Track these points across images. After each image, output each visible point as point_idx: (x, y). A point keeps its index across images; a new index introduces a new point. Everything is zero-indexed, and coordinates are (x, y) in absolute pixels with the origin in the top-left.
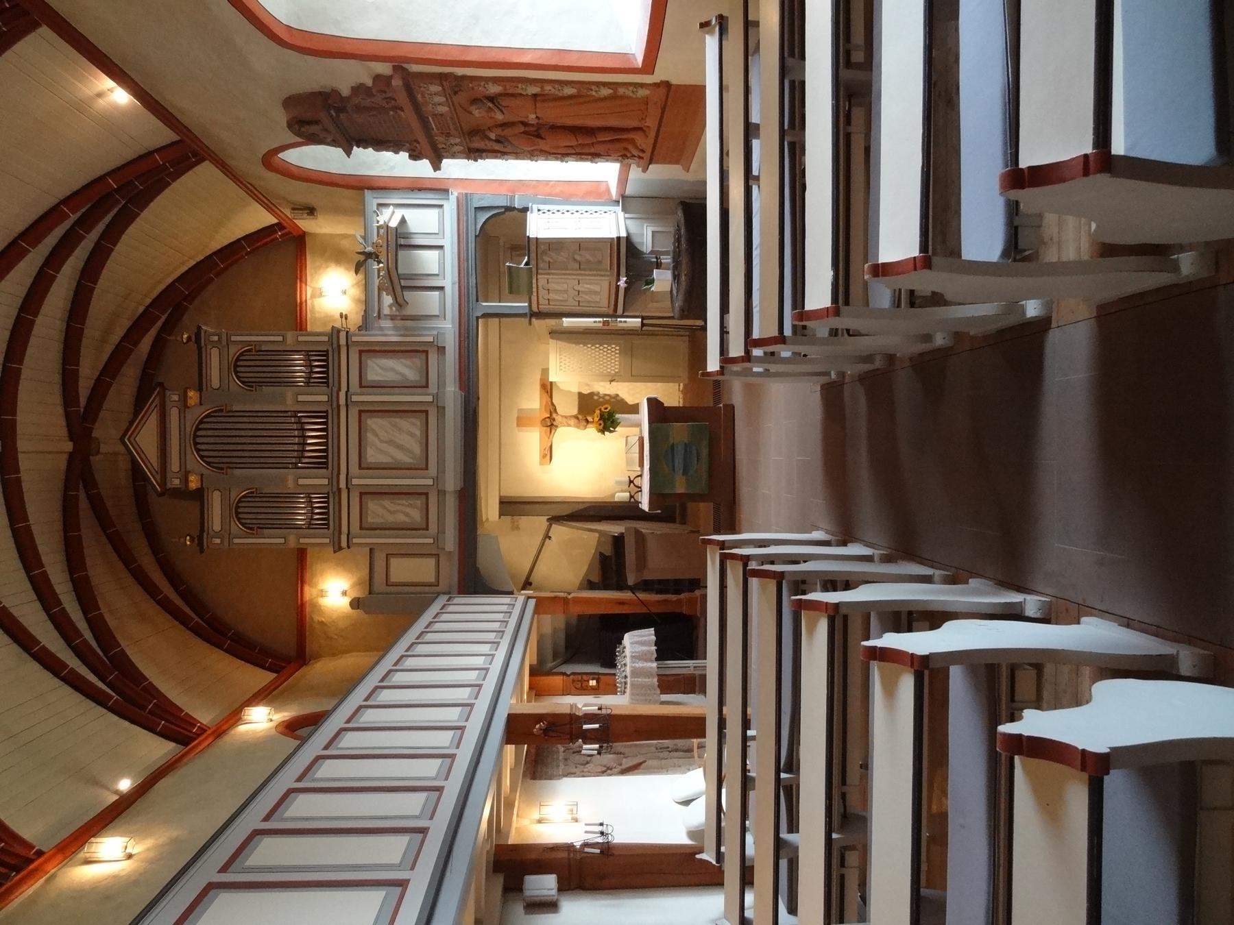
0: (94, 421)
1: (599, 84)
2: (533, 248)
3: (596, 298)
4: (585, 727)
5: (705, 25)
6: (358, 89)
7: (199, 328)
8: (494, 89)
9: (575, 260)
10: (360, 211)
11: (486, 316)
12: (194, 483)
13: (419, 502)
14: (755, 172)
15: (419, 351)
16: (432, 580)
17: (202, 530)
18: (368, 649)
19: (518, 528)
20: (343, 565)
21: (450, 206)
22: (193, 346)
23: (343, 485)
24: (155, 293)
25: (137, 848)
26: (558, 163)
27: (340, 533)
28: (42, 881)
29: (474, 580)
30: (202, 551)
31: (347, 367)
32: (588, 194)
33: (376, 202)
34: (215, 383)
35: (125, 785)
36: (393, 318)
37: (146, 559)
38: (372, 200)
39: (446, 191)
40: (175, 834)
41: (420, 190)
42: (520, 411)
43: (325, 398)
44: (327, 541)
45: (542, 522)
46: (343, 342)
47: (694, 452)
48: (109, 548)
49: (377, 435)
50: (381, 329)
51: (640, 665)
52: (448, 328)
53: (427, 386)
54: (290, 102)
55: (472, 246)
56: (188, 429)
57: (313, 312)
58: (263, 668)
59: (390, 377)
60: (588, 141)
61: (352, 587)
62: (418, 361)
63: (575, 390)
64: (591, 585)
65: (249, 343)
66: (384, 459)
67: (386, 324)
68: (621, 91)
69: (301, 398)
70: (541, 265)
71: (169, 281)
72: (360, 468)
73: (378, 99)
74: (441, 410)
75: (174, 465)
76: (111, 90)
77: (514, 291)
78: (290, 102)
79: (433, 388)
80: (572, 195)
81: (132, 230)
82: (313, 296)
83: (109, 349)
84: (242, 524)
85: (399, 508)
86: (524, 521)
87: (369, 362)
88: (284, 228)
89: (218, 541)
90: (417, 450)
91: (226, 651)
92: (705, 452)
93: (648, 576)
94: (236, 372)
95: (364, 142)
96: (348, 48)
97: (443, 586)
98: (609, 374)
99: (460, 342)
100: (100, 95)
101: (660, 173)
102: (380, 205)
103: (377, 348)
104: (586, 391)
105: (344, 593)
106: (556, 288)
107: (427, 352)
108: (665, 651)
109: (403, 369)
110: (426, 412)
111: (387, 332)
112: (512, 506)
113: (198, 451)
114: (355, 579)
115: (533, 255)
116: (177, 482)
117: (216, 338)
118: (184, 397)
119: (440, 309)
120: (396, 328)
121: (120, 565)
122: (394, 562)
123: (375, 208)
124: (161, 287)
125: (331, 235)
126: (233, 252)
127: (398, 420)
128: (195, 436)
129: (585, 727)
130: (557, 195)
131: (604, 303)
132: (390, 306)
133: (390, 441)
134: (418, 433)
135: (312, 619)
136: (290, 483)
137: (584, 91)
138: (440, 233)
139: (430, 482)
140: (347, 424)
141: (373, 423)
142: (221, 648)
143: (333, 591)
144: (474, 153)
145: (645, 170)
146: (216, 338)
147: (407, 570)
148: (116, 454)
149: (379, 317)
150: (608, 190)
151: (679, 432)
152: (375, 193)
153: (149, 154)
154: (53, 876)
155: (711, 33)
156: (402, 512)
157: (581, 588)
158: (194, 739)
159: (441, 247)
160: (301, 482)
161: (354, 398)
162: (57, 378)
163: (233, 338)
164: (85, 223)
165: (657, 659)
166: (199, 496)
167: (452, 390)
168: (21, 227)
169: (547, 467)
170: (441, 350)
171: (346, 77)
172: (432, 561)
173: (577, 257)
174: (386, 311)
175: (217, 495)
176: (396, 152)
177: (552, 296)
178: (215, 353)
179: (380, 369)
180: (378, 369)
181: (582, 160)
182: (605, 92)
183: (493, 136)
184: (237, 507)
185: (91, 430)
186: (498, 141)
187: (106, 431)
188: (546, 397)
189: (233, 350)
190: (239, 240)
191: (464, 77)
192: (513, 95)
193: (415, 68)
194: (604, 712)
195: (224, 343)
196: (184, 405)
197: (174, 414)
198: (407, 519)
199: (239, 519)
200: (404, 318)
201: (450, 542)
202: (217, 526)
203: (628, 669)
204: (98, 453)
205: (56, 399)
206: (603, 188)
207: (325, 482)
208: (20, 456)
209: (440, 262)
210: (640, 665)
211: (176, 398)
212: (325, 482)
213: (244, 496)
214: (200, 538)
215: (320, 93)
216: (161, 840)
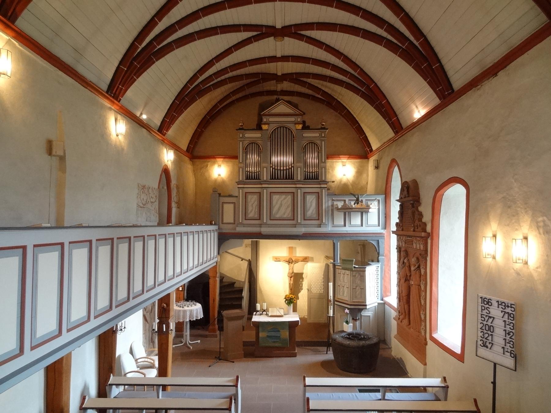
1: (425, 315)
2: (361, 269)
3: (341, 293)
4: (164, 325)
5: (445, 378)
6: (421, 215)
7: (327, 129)
8: (423, 271)
9: (356, 287)
10: (377, 193)
12: (265, 127)
13: (257, 216)
14: (389, 395)
15: (319, 216)
16: (225, 221)
18: (196, 185)
19: (246, 247)
20: (232, 173)
21: (379, 230)
22: (320, 127)
23: (264, 186)
25: (121, 138)
26: (396, 283)
28: (109, 106)
29: (223, 239)
30: (237, 130)
31: (312, 187)
32: (385, 287)
34: (305, 135)
35: (144, 117)
36: (332, 205)
37: (234, 98)
38: (381, 198)
40: (125, 148)
41: (386, 217)
42: (296, 248)
43: (299, 179)
44: (241, 179)
45: (249, 257)
46: (322, 186)
47: (275, 340)
48: (238, 87)
49: (284, 199)
50: (328, 201)
51: (188, 314)
52: (329, 229)
54: (415, 182)
55: (363, 239)
58: (189, 144)
60: (405, 301)
61: (222, 178)
62: (315, 216)
63: (304, 272)
64: (221, 281)
65: (321, 149)
66: (274, 202)
67: (330, 204)
68: (423, 324)
69: (299, 169)
70: (354, 273)
72: (271, 193)
73: (417, 222)
74: (295, 226)
75: (272, 119)
76: (419, 112)
77: (344, 261)
78: (415, 182)
80: (385, 281)
81: (365, 102)
82: (342, 162)
83: (320, 86)
85: (254, 209)
86: (249, 249)
87: (314, 196)
89: (241, 136)
90: (278, 216)
92: (277, 345)
93: (225, 320)
95: (401, 206)
96: (436, 218)
97: (222, 226)
98: (311, 288)
101: (394, 325)
102: (379, 201)
104: (304, 276)
105: (219, 175)
106: (345, 278)
107: (318, 219)
108: (194, 324)
109: (311, 210)
110: (294, 220)
111: (326, 203)
112: (255, 249)
113: (278, 128)
114: (225, 179)
115: (358, 269)
116: (265, 120)
118: (299, 123)
119: (336, 225)
120: (328, 207)
122: (232, 205)
124: (345, 105)
125: (368, 170)
126: (360, 131)
127: (290, 208)
128: (283, 127)
129: (164, 325)
130: (384, 274)
131: (339, 297)
134: (285, 216)
135: (209, 162)
136: (264, 165)
137: (423, 308)
138: (368, 226)
139: (265, 221)
140: (288, 187)
141: (289, 197)
143: (220, 171)
144: (399, 249)
145: (394, 319)
146: (323, 135)
148: (277, 87)
150: (387, 296)
151: (285, 334)
153: (396, 116)
154: (110, 109)
155: (442, 382)
156: (252, 210)
157: (221, 273)
158: (161, 133)
159: (362, 226)
160: (265, 169)
161: (299, 191)
163: (323, 142)
165: (190, 321)
166: (259, 127)
167: (302, 230)
168: (365, 69)
169: (272, 259)
170: (319, 226)
171: (425, 209)
172: (232, 221)
173: (358, 288)
174: (335, 203)
176: (398, 218)
177: (342, 275)
178: (317, 135)
180: (311, 200)
181: (398, 293)
182: (423, 317)
183: (405, 261)
185: (286, 81)
186: (404, 262)
188: (301, 259)
189: (318, 142)
191: (426, 260)
192: (420, 277)
193: (429, 241)
194: (170, 332)
196: (296, 123)
197: (292, 119)
198: (249, 211)
201: (240, 229)
202: (246, 135)
203: (186, 308)
206: (388, 294)
207: (265, 179)
209: (355, 225)
210: (188, 314)
211: (299, 120)
212: (265, 179)
214: (242, 129)
215: (419, 198)
216: (123, 144)
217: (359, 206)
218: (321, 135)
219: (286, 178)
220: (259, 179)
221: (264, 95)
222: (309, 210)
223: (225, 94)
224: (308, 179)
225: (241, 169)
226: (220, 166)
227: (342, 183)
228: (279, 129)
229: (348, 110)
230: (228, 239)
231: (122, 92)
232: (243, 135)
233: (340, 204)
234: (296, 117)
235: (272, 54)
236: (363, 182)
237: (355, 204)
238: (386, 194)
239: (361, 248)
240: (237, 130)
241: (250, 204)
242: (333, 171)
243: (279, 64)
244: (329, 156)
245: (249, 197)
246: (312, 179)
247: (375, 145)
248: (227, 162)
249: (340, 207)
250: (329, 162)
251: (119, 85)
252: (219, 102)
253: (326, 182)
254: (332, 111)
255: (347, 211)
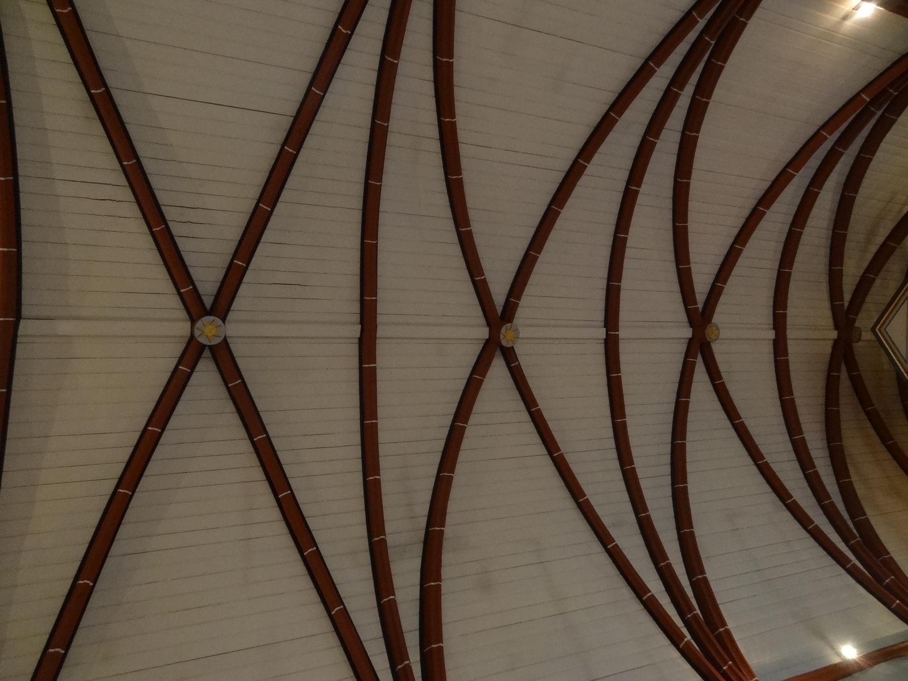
0: (857, 314)
76: (856, 8)
100: (846, 17)
121: (877, 439)
162: (824, 279)
164: (844, 141)
185: (854, 321)
187: (864, 321)
204: (859, 340)
205: (823, 295)
208: (789, 342)
223: (887, 455)
231: (734, 668)
235: (768, 348)
243: (791, 334)
251: (719, 668)
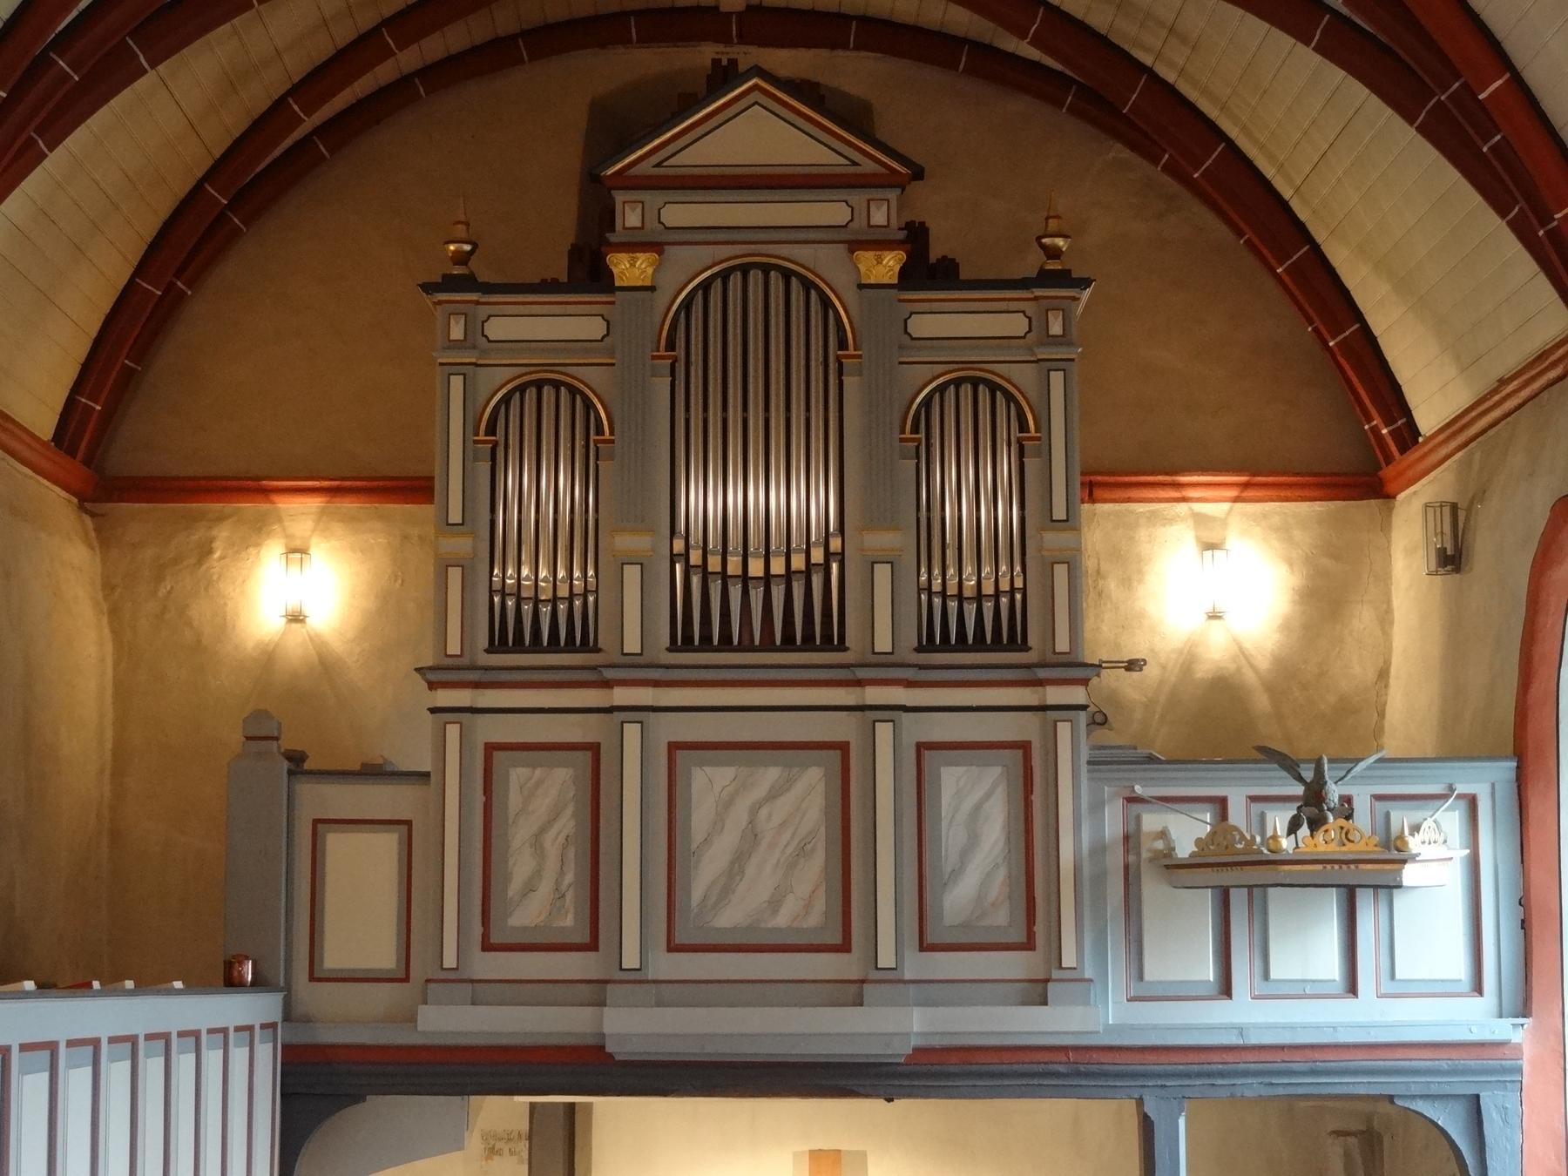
7: (1084, 283)
10: (1457, 747)
11: (1147, 1127)
12: (629, 268)
13: (569, 922)
15: (1032, 917)
16: (332, 959)
17: (489, 289)
18: (123, 692)
19: (492, 1152)
20: (386, 608)
21: (1476, 1019)
22: (1031, 264)
23: (621, 696)
24: (1192, 95)
27: (477, 685)
30: (429, 288)
31: (979, 707)
33: (1482, 791)
34: (923, 326)
36: (1130, 840)
38: (1487, 781)
39: (1524, 1009)
41: (1525, 924)
42: (862, 1156)
43: (883, 643)
44: (454, 648)
46: (1055, 695)
49: (773, 795)
50: (1097, 807)
52: (1106, 1013)
53: (924, 947)
56: (784, 250)
57: (1153, 518)
59: (950, 836)
61: (317, 642)
62: (1003, 920)
65: (1044, 423)
66: (700, 817)
67: (1112, 823)
69: (882, 573)
71: (1233, 132)
72: (674, 747)
74: (853, 993)
75: (681, 213)
79: (917, 965)
81: (1359, 92)
82: (1200, 520)
84: (506, 400)
87: (996, 771)
88: (1403, 449)
89: (457, 332)
90: (729, 918)
91: (129, 289)
94: (957, 383)
97: (312, 996)
99: (1064, 1049)
102: (1472, 802)
103: (1037, 798)
105: (296, 618)
107: (1029, 945)
109: (976, 875)
110: (845, 947)
111: (1085, 822)
113: (725, 275)
114: (337, 645)
116: (633, 219)
117: (1056, 328)
118: (880, 244)
119: (1163, 986)
120: (1099, 850)
122: (386, 844)
123: (1461, 789)
125: (1384, 578)
128: (766, 269)
132: (1163, 834)
133: (754, 836)
134: (782, 920)
135: (221, 518)
136: (627, 542)
138: (1395, 988)
139: (631, 959)
141: (811, 784)
142: (141, 269)
143: (301, 587)
146: (1056, 328)
147: (360, 889)
149: (1133, 800)
152: (1506, 792)
156: (538, 874)
159: (1352, 988)
160: (632, 574)
161: (884, 732)
163: (1057, 378)
167: (907, 1025)
170: (1037, 992)
172: (385, 957)
174: (1151, 821)
175: (592, 328)
178: (1015, 324)
179: (973, 802)
180: (973, 802)
184: (557, 385)
189: (1023, 377)
190: (1358, 316)
195: (1042, 353)
197: (830, 211)
199: (522, 389)
200: (1130, 877)
201: (447, 1022)
202: (498, 329)
207: (632, 644)
209: (1301, 987)
211: (879, 217)
212: (632, 644)
213: (589, 405)
214: (467, 283)
217: (1323, 843)
218: (1037, 326)
219: (789, 643)
220: (587, 646)
221: (627, 42)
222: (957, 873)
223: (345, 34)
224: (946, 646)
225: (455, 575)
226: (298, 550)
227: (1202, 671)
228: (735, 280)
229: (1231, 144)
230: (358, 1098)
232: (475, 330)
233: (1187, 833)
234: (858, 198)
236: (1356, 669)
237: (1293, 828)
238: (1520, 754)
239: (1347, 1155)
240: (429, 288)
241: (520, 834)
242: (1127, 583)
244: (1103, 480)
245: (516, 775)
246: (980, 644)
247: (1433, 400)
248: (349, 520)
249: (1185, 849)
250: (1102, 522)
252: (295, 90)
253: (1077, 669)
254: (1120, 152)
255: (1238, 882)
